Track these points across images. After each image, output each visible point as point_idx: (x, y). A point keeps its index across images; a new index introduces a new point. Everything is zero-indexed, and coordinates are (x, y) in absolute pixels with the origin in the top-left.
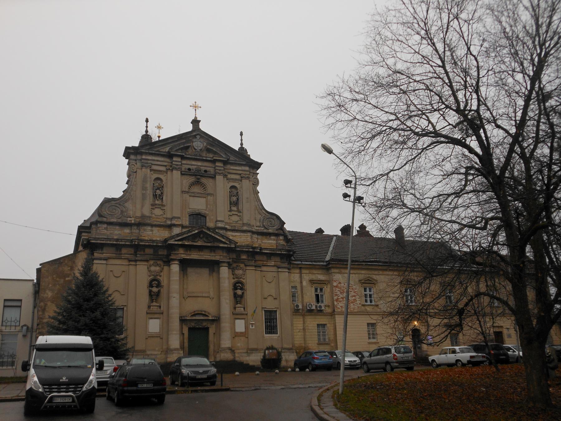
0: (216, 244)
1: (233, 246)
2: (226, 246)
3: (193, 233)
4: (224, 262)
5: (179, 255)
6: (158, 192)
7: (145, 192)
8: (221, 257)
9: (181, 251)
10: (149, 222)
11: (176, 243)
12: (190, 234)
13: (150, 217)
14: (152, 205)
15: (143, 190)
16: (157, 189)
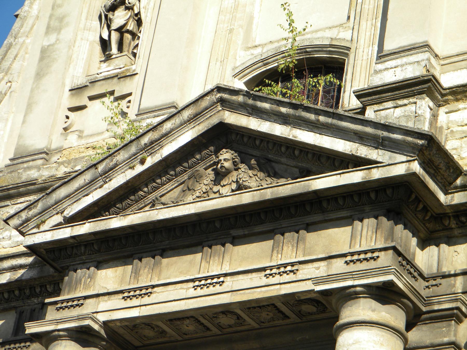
0: (287, 188)
1: (398, 166)
2: (355, 177)
3: (169, 149)
4: (347, 295)
5: (89, 307)
6: (120, 17)
7: (53, 38)
8: (339, 266)
9: (109, 278)
10: (33, 174)
11: (66, 233)
12: (150, 162)
13: (46, 154)
14: (77, 90)
15: (49, 30)
16: (113, 8)
